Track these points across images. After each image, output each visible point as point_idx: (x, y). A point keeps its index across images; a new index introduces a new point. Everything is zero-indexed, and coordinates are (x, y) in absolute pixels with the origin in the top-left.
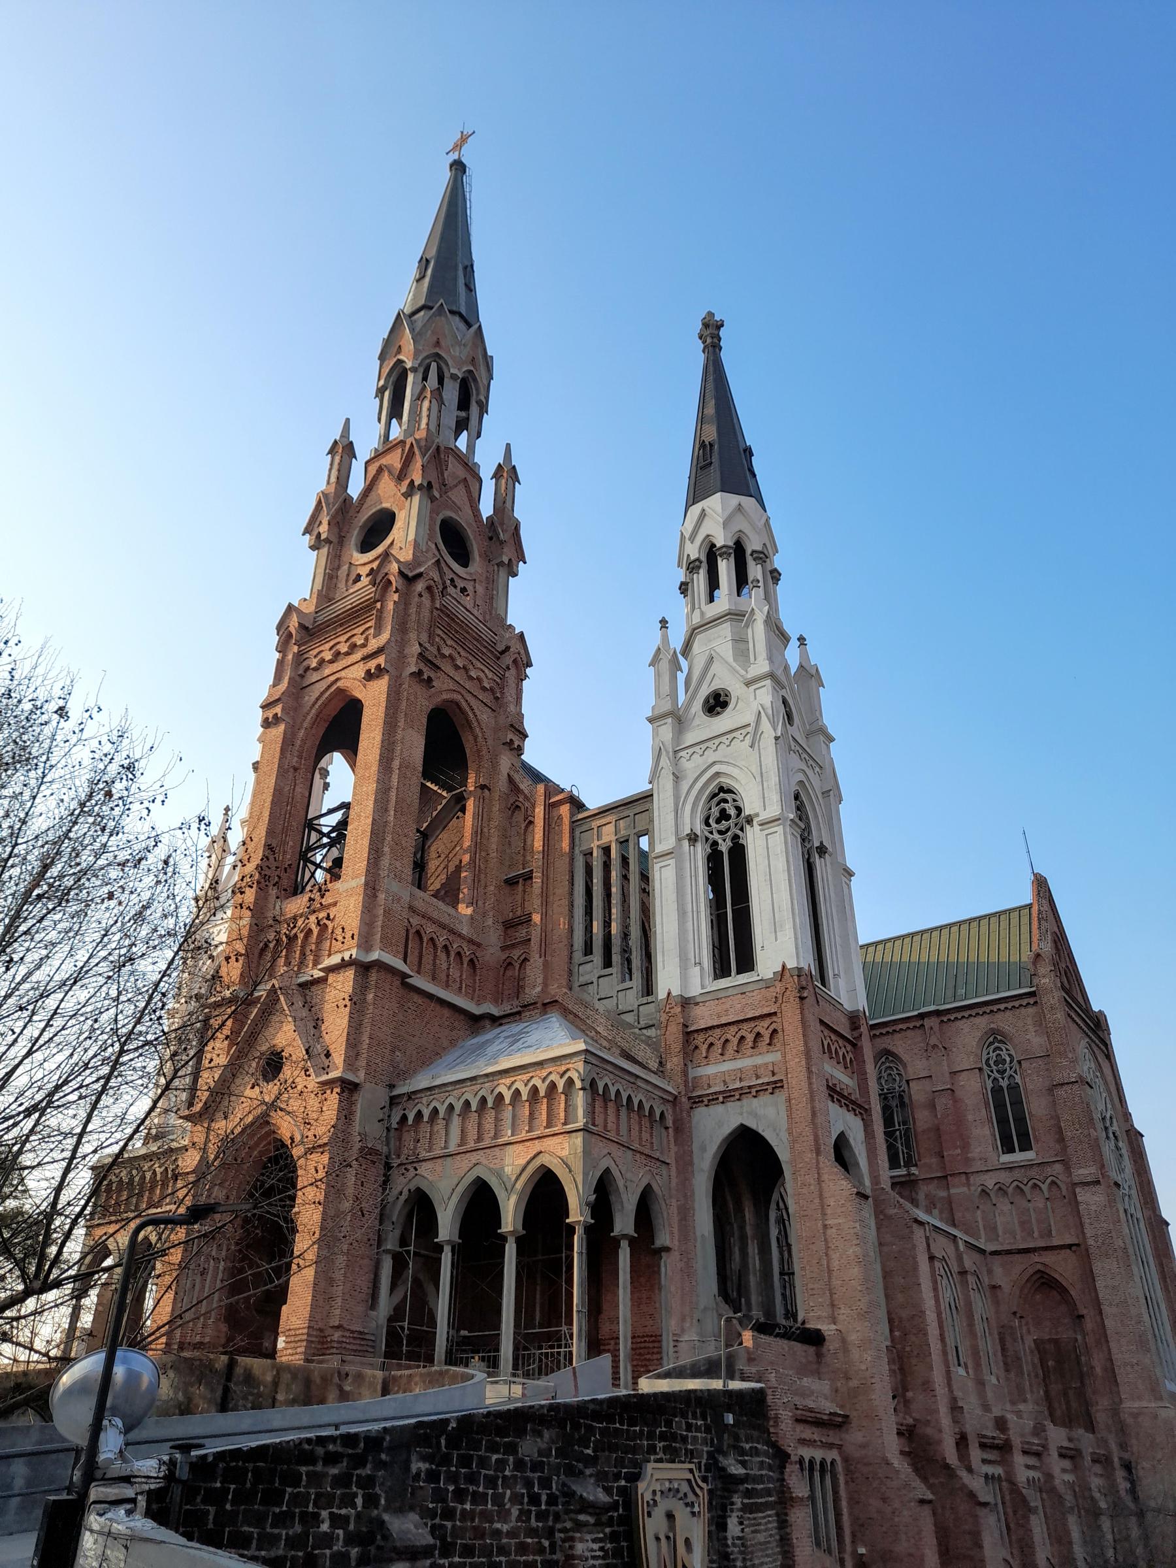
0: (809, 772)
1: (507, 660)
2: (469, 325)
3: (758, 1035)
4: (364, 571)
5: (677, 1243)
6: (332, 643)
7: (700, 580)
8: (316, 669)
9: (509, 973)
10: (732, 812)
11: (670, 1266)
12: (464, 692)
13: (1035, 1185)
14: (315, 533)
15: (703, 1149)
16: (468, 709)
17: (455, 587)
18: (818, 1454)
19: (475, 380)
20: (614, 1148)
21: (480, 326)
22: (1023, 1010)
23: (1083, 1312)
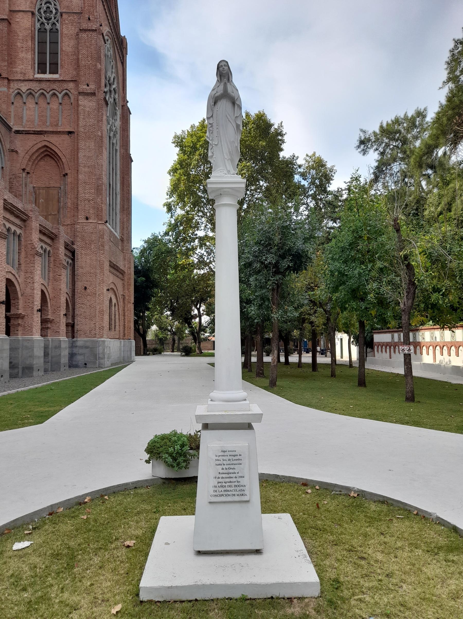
23: (68, 171)
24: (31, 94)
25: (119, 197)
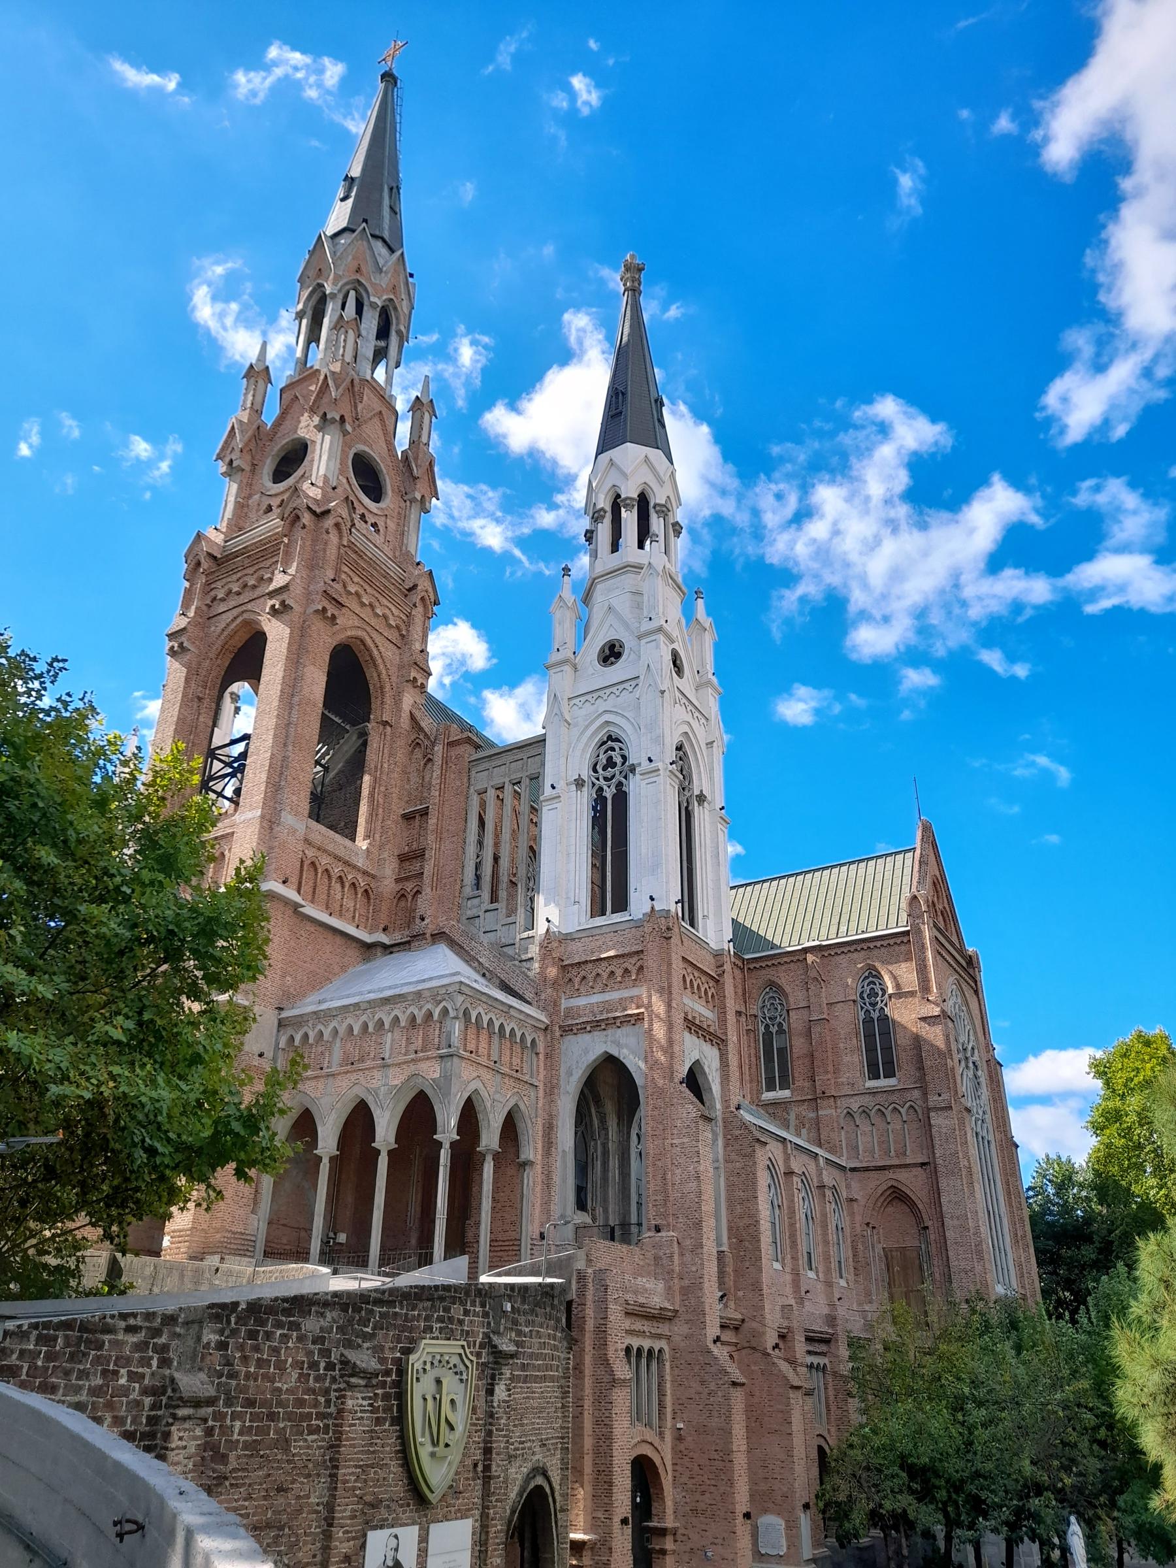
0: (695, 724)
1: (416, 597)
2: (392, 251)
3: (626, 971)
4: (275, 502)
5: (539, 1157)
6: (239, 575)
7: (604, 531)
8: (223, 600)
9: (402, 904)
10: (619, 760)
11: (532, 1179)
12: (369, 629)
13: (895, 1108)
14: (227, 460)
15: (570, 1073)
16: (372, 646)
17: (366, 522)
18: (646, 1344)
19: (395, 309)
20: (483, 1072)
21: (402, 254)
22: (896, 947)
23: (929, 1223)
24: (865, 1112)
25: (1005, 1221)
